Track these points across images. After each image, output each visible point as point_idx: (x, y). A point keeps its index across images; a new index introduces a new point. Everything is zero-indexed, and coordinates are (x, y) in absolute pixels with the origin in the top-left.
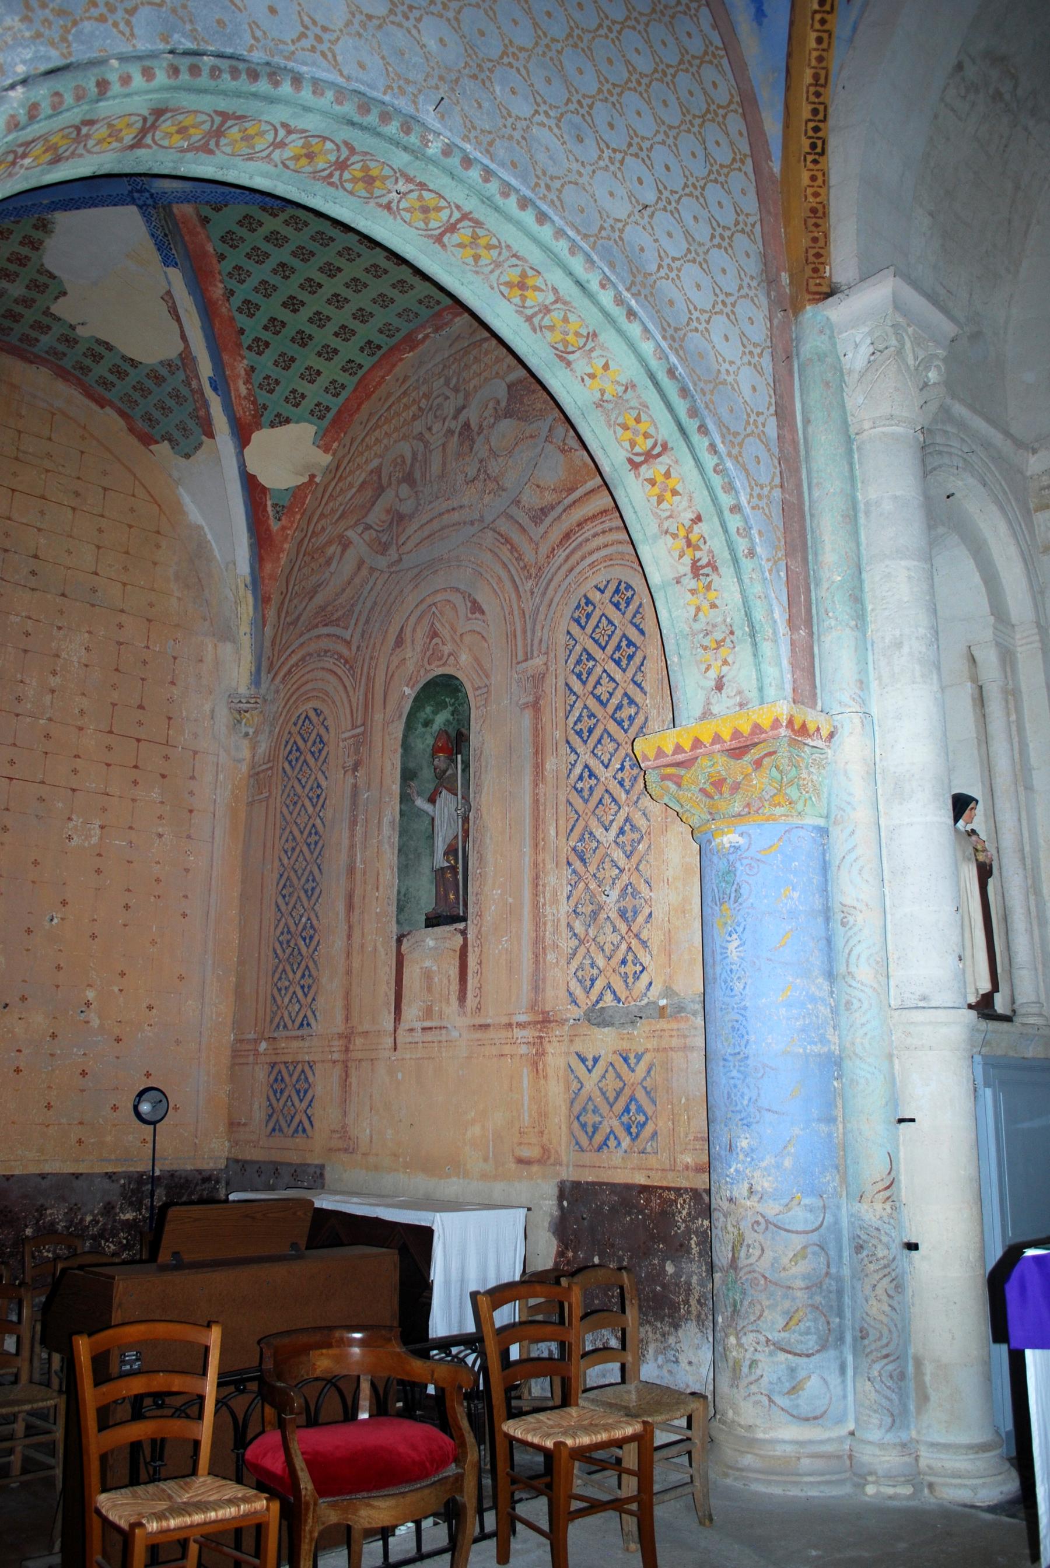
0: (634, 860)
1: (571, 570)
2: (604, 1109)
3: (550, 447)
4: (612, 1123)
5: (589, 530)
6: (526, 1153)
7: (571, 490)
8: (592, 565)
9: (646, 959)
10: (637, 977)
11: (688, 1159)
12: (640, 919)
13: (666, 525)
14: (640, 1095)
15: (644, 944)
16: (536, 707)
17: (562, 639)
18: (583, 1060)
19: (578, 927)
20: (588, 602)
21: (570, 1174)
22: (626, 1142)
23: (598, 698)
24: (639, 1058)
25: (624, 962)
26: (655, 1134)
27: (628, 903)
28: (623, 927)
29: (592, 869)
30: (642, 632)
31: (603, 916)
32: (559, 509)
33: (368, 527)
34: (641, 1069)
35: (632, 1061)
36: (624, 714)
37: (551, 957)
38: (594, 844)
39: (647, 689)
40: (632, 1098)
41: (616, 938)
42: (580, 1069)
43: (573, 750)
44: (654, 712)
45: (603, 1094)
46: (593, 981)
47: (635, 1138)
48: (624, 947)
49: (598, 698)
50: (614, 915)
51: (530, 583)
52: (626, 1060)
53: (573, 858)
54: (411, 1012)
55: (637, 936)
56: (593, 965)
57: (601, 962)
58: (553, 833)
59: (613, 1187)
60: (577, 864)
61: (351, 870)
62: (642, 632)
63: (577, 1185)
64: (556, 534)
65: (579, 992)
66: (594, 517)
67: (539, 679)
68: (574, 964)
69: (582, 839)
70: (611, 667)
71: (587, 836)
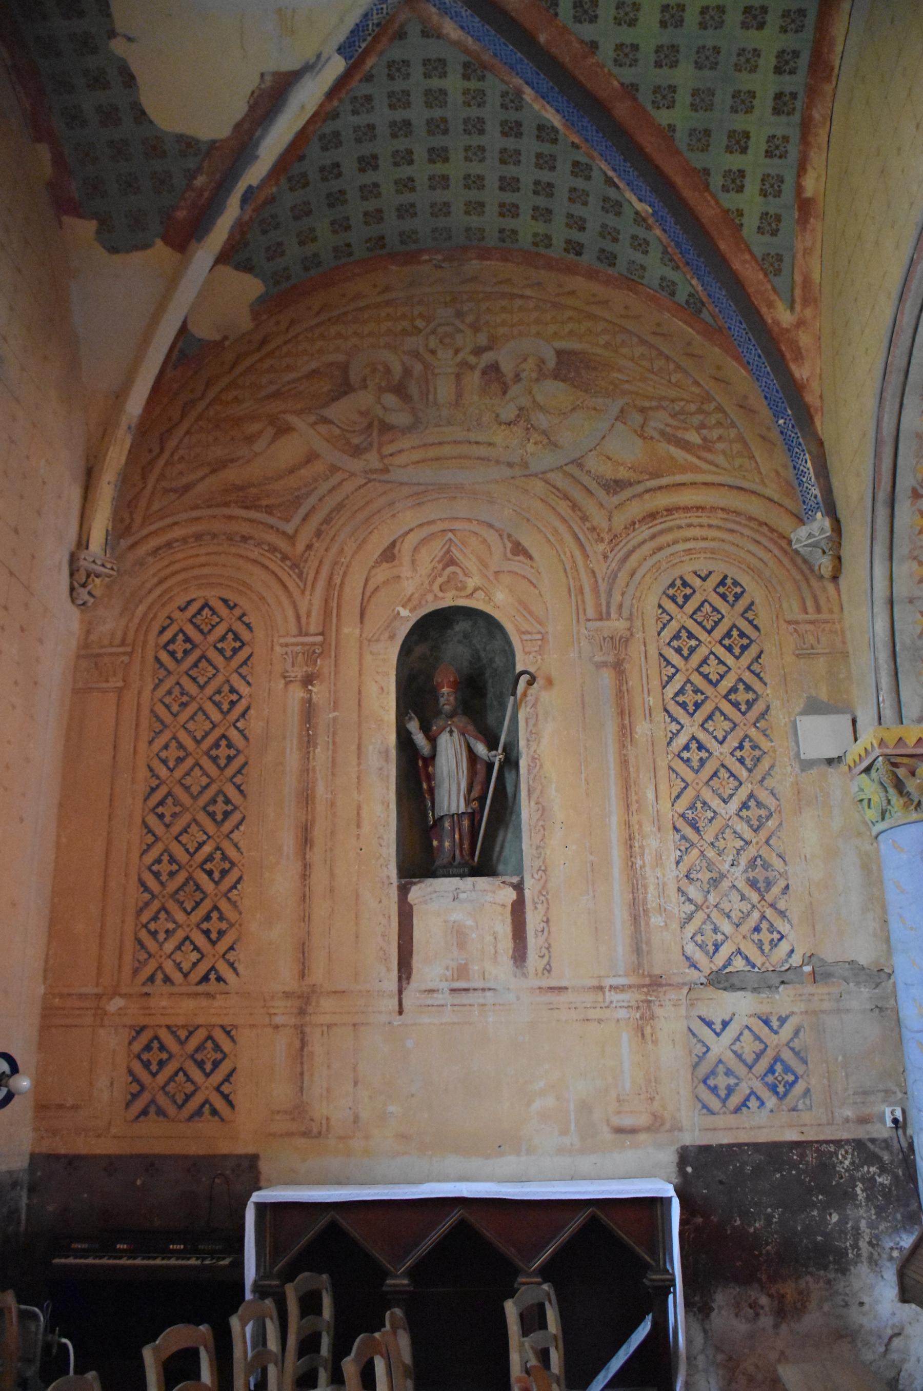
0: (763, 834)
1: (660, 549)
2: (741, 1070)
3: (620, 426)
4: (750, 1083)
5: (680, 519)
6: (627, 1121)
7: (654, 475)
8: (688, 551)
9: (784, 928)
10: (774, 944)
11: (849, 1113)
12: (776, 890)
13: (916, 553)
14: (787, 1055)
15: (782, 914)
16: (618, 667)
17: (651, 611)
18: (709, 1024)
19: (693, 892)
20: (685, 584)
21: (692, 1138)
22: (771, 1101)
23: (706, 677)
24: (782, 1020)
25: (757, 929)
26: (807, 1092)
27: (759, 874)
28: (755, 897)
29: (709, 837)
30: (756, 628)
31: (726, 884)
32: (639, 488)
33: (326, 421)
34: (786, 1032)
35: (775, 1024)
36: (742, 696)
37: (656, 920)
38: (710, 814)
39: (766, 679)
40: (777, 1059)
41: (746, 907)
42: (705, 1033)
43: (674, 719)
44: (776, 704)
45: (739, 1056)
46: (717, 947)
47: (781, 1098)
48: (756, 915)
49: (706, 677)
50: (741, 884)
51: (601, 547)
52: (766, 1022)
53: (681, 824)
54: (429, 970)
55: (772, 906)
56: (715, 930)
57: (727, 927)
58: (650, 795)
59: (757, 1147)
60: (688, 831)
61: (306, 797)
62: (756, 628)
63: (705, 1149)
64: (636, 509)
65: (698, 956)
66: (686, 509)
67: (620, 643)
68: (691, 929)
69: (693, 807)
70: (721, 651)
71: (699, 805)
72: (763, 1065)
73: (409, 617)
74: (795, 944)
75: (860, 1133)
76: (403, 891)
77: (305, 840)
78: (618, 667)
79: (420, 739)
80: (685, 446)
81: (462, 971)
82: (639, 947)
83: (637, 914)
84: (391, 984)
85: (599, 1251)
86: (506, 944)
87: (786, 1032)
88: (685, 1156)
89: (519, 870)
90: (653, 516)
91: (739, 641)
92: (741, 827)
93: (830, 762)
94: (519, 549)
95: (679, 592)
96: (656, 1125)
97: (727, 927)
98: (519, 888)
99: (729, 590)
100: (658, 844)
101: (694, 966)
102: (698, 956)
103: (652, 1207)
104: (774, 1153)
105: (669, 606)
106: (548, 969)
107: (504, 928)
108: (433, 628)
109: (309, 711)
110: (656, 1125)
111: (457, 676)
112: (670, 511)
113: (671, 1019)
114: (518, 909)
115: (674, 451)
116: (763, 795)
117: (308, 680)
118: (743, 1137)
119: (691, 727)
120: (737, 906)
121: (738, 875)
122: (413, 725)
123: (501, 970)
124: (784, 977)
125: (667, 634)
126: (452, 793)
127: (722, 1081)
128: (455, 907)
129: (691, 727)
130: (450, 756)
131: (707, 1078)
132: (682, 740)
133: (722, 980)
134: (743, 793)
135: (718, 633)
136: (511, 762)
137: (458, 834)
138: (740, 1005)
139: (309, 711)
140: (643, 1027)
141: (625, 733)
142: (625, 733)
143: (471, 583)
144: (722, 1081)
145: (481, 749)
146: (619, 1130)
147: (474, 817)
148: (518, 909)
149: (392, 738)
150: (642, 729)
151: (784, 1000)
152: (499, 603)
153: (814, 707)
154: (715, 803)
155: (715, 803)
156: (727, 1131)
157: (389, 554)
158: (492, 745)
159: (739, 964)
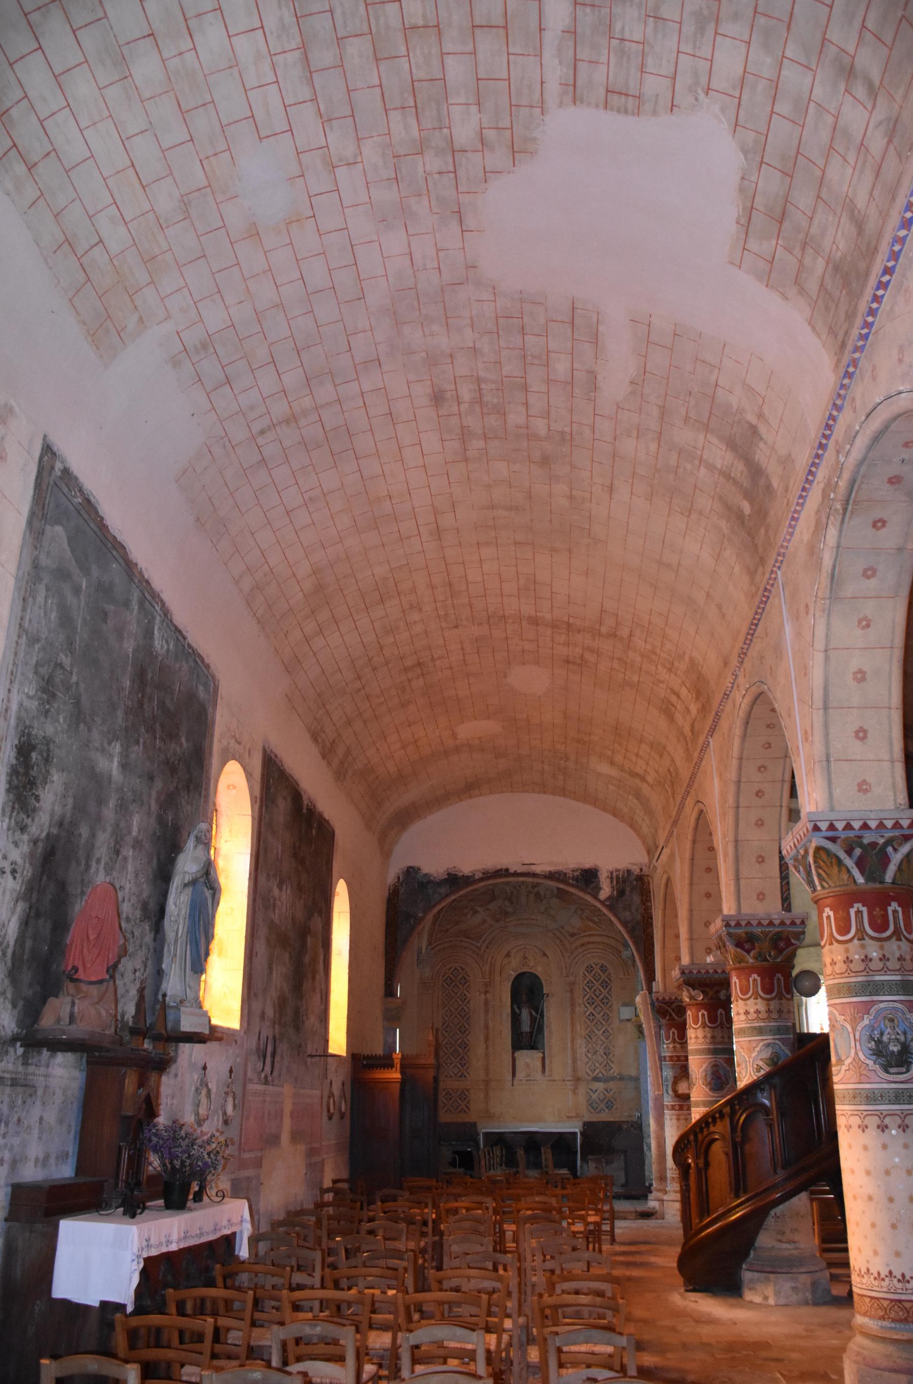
2: (599, 1102)
4: (602, 1106)
5: (591, 946)
6: (571, 1115)
16: (571, 991)
17: (581, 974)
19: (589, 1055)
21: (586, 1119)
22: (607, 1111)
27: (607, 1051)
33: (488, 909)
34: (611, 1093)
36: (605, 1001)
42: (592, 1094)
54: (520, 1074)
57: (597, 1065)
59: (603, 1122)
61: (487, 1027)
64: (579, 942)
65: (590, 1073)
67: (572, 984)
70: (600, 987)
72: (605, 1101)
73: (514, 974)
74: (615, 1071)
75: (629, 1119)
76: (513, 1053)
77: (487, 1039)
78: (571, 991)
79: (517, 1010)
80: (594, 922)
81: (528, 1075)
82: (575, 1069)
83: (574, 1061)
84: (510, 1078)
85: (561, 1144)
86: (540, 1068)
87: (611, 1093)
88: (585, 1124)
89: (544, 1048)
90: (583, 945)
91: (605, 984)
92: (602, 1038)
93: (628, 1020)
94: (545, 955)
95: (590, 969)
96: (577, 1116)
97: (597, 1065)
98: (543, 1053)
99: (603, 968)
100: (581, 1043)
101: (588, 1075)
102: (590, 1073)
103: (575, 1134)
104: (607, 1124)
105: (586, 973)
106: (551, 1076)
107: (539, 1064)
108: (520, 977)
109: (486, 1002)
110: (577, 1116)
111: (528, 992)
112: (589, 943)
113: (582, 1089)
114: (543, 1059)
115: (591, 924)
116: (609, 1029)
117: (486, 992)
118: (600, 1120)
119: (591, 1010)
120: (601, 1060)
121: (601, 1051)
122: (515, 1007)
123: (538, 1075)
124: (613, 1078)
125: (586, 981)
126: (526, 1027)
127: (595, 1105)
128: (528, 1059)
129: (591, 1010)
130: (525, 1014)
131: (591, 1104)
132: (588, 1013)
133: (596, 1079)
134: (604, 1029)
135: (600, 981)
136: (542, 1016)
137: (528, 1038)
138: (600, 1086)
139: (486, 1002)
140: (575, 1091)
141: (573, 1011)
142: (573, 1011)
143: (531, 964)
144: (595, 1105)
145: (534, 1013)
146: (569, 1117)
147: (531, 1033)
148: (543, 1059)
149: (509, 1010)
150: (577, 1009)
151: (611, 1085)
152: (539, 971)
153: (625, 1004)
154: (596, 1031)
155: (596, 1031)
156: (596, 1118)
157: (508, 955)
158: (537, 1013)
159: (600, 1075)
